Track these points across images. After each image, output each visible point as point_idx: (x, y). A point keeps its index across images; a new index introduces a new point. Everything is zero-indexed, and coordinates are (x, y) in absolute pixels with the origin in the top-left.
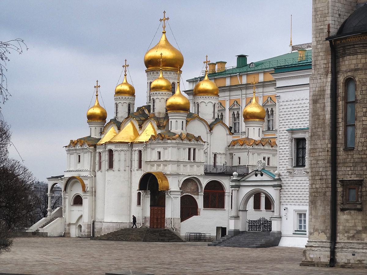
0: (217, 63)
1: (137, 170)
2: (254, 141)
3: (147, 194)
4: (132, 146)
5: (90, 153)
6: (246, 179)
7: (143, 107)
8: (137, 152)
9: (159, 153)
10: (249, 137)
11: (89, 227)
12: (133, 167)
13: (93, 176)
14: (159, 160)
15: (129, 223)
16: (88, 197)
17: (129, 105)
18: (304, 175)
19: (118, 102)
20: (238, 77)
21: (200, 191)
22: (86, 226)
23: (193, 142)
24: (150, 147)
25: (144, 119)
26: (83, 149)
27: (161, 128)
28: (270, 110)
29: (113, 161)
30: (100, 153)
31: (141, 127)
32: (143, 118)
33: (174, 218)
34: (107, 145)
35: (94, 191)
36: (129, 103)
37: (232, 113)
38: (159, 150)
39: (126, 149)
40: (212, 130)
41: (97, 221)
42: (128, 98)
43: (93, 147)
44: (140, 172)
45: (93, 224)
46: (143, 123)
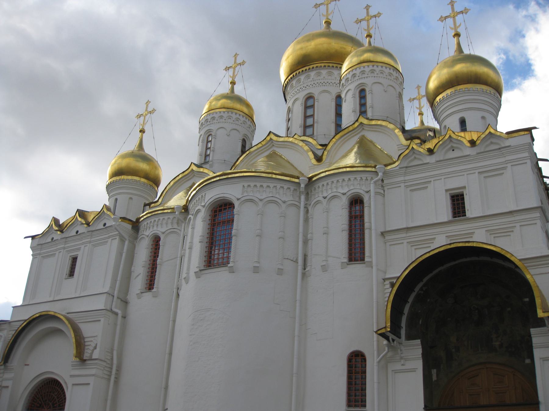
1: (343, 266)
3: (401, 358)
5: (116, 242)
8: (344, 202)
12: (315, 262)
13: (119, 312)
16: (91, 380)
17: (244, 141)
19: (214, 127)
24: (405, 181)
26: (92, 231)
29: (230, 238)
34: (191, 206)
35: (115, 362)
36: (245, 135)
38: (455, 184)
43: (129, 227)
44: (357, 268)
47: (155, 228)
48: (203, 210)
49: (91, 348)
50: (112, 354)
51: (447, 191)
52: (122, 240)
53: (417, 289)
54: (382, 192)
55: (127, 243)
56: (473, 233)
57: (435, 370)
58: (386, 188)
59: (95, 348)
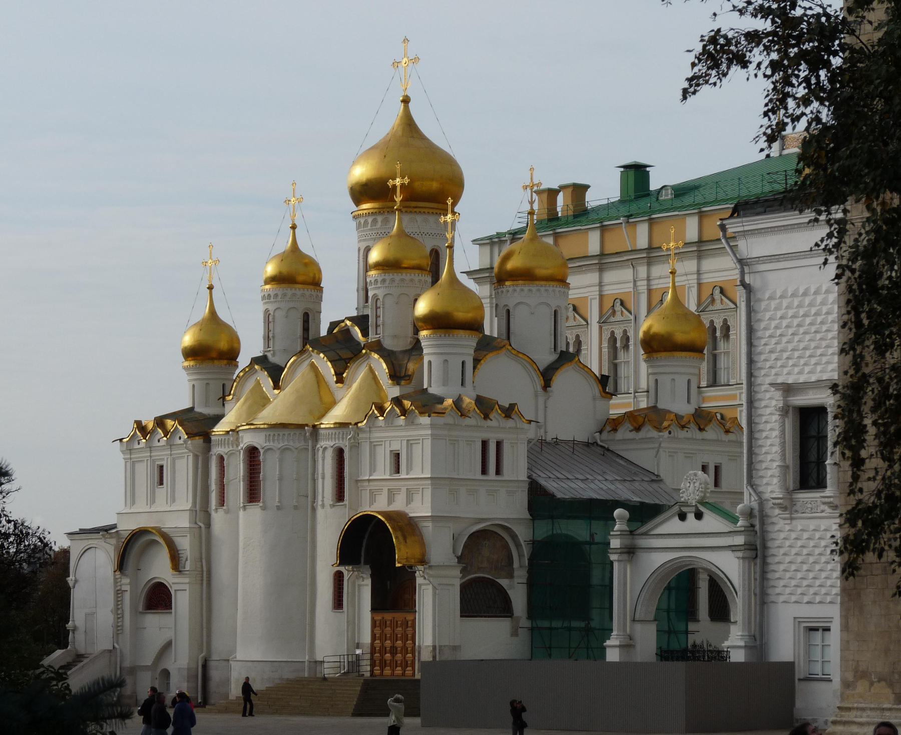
0: (563, 188)
1: (332, 506)
2: (672, 416)
4: (316, 435)
5: (191, 458)
6: (656, 527)
7: (348, 323)
9: (397, 456)
10: (660, 406)
11: (192, 677)
14: (396, 476)
15: (310, 662)
18: (823, 514)
20: (624, 229)
21: (516, 564)
22: (185, 673)
23: (493, 423)
25: (349, 355)
27: (403, 382)
28: (718, 324)
30: (221, 459)
31: (340, 380)
32: (345, 354)
33: (440, 646)
35: (205, 569)
37: (606, 336)
38: (396, 446)
39: (297, 445)
40: (550, 387)
41: (215, 657)
42: (303, 295)
45: (205, 666)
46: (346, 368)
47: (220, 449)
48: (242, 452)
49: (184, 560)
50: (201, 561)
51: (391, 451)
52: (196, 457)
53: (369, 529)
54: (357, 445)
55: (200, 459)
56: (400, 489)
57: (389, 582)
58: (360, 441)
59: (187, 560)
